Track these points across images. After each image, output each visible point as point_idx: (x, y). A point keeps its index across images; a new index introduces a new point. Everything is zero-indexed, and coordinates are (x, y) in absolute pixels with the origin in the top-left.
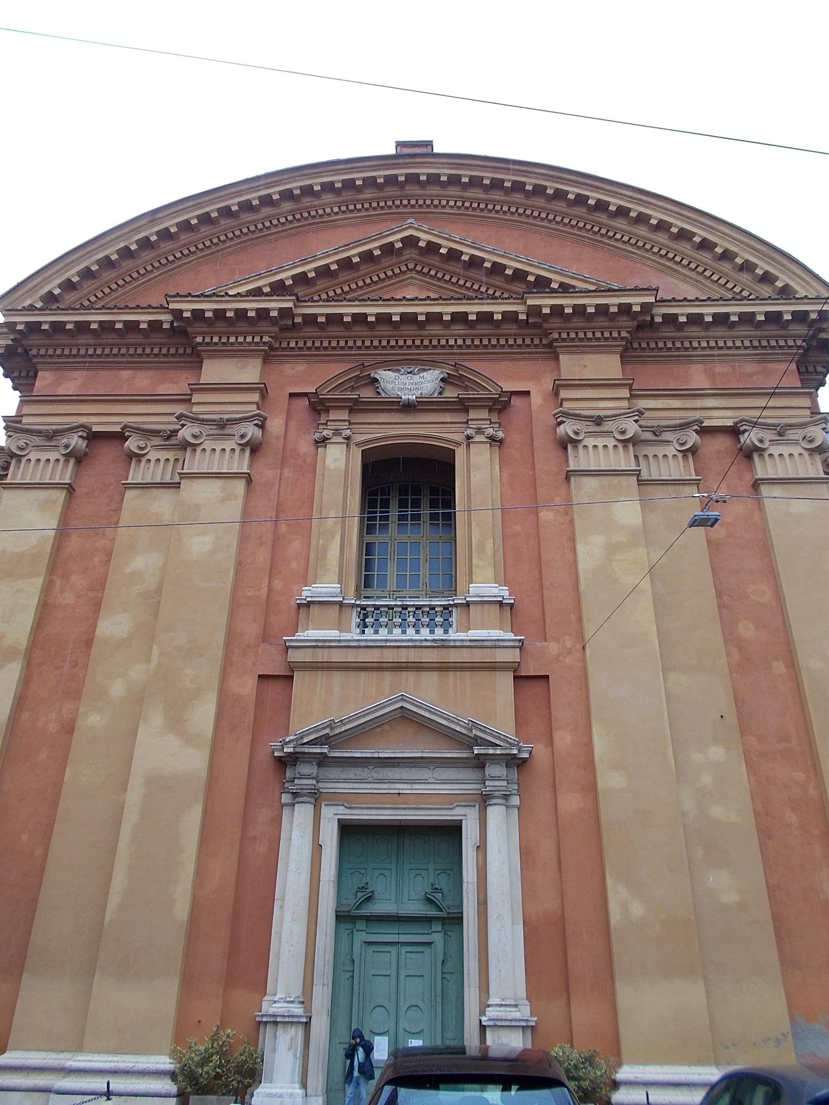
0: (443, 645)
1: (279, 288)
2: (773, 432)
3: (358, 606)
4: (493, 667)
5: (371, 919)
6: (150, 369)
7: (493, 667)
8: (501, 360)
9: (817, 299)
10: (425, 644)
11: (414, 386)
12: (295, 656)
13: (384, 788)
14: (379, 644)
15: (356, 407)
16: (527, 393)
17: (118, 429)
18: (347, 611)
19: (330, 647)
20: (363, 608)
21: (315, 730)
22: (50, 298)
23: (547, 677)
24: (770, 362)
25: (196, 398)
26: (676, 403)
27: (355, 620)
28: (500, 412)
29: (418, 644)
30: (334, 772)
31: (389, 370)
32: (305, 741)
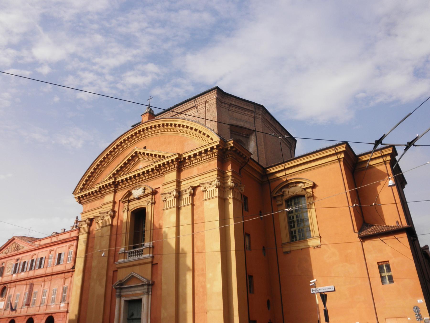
0: (139, 260)
1: (110, 178)
2: (208, 184)
3: (128, 252)
4: (147, 263)
5: (133, 319)
6: (99, 200)
7: (147, 263)
8: (155, 179)
9: (215, 142)
10: (136, 260)
11: (139, 193)
12: (118, 266)
13: (130, 293)
14: (129, 261)
15: (129, 201)
16: (159, 188)
17: (93, 217)
18: (126, 254)
19: (122, 263)
20: (129, 252)
21: (117, 283)
22: (81, 189)
23: (157, 264)
24: (211, 161)
25: (103, 207)
26: (189, 181)
27: (128, 255)
29: (135, 260)
30: (124, 290)
31: (134, 190)
32: (116, 285)
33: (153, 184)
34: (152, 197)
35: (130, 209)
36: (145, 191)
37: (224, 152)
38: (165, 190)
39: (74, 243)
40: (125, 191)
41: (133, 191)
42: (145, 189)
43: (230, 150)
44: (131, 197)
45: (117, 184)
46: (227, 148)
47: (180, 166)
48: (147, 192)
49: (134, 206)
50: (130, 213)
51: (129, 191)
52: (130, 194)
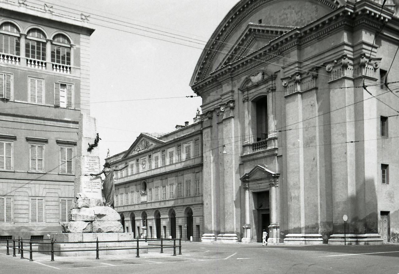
15: (248, 89)
16: (280, 71)
17: (213, 109)
25: (223, 98)
28: (275, 79)
33: (272, 67)
34: (272, 82)
35: (250, 98)
36: (264, 77)
37: (354, 18)
38: (286, 74)
39: (199, 136)
40: (243, 78)
41: (252, 78)
42: (263, 74)
43: (361, 15)
44: (250, 84)
45: (233, 71)
46: (358, 12)
47: (301, 43)
48: (266, 77)
49: (254, 93)
50: (250, 103)
51: (247, 78)
52: (248, 80)
